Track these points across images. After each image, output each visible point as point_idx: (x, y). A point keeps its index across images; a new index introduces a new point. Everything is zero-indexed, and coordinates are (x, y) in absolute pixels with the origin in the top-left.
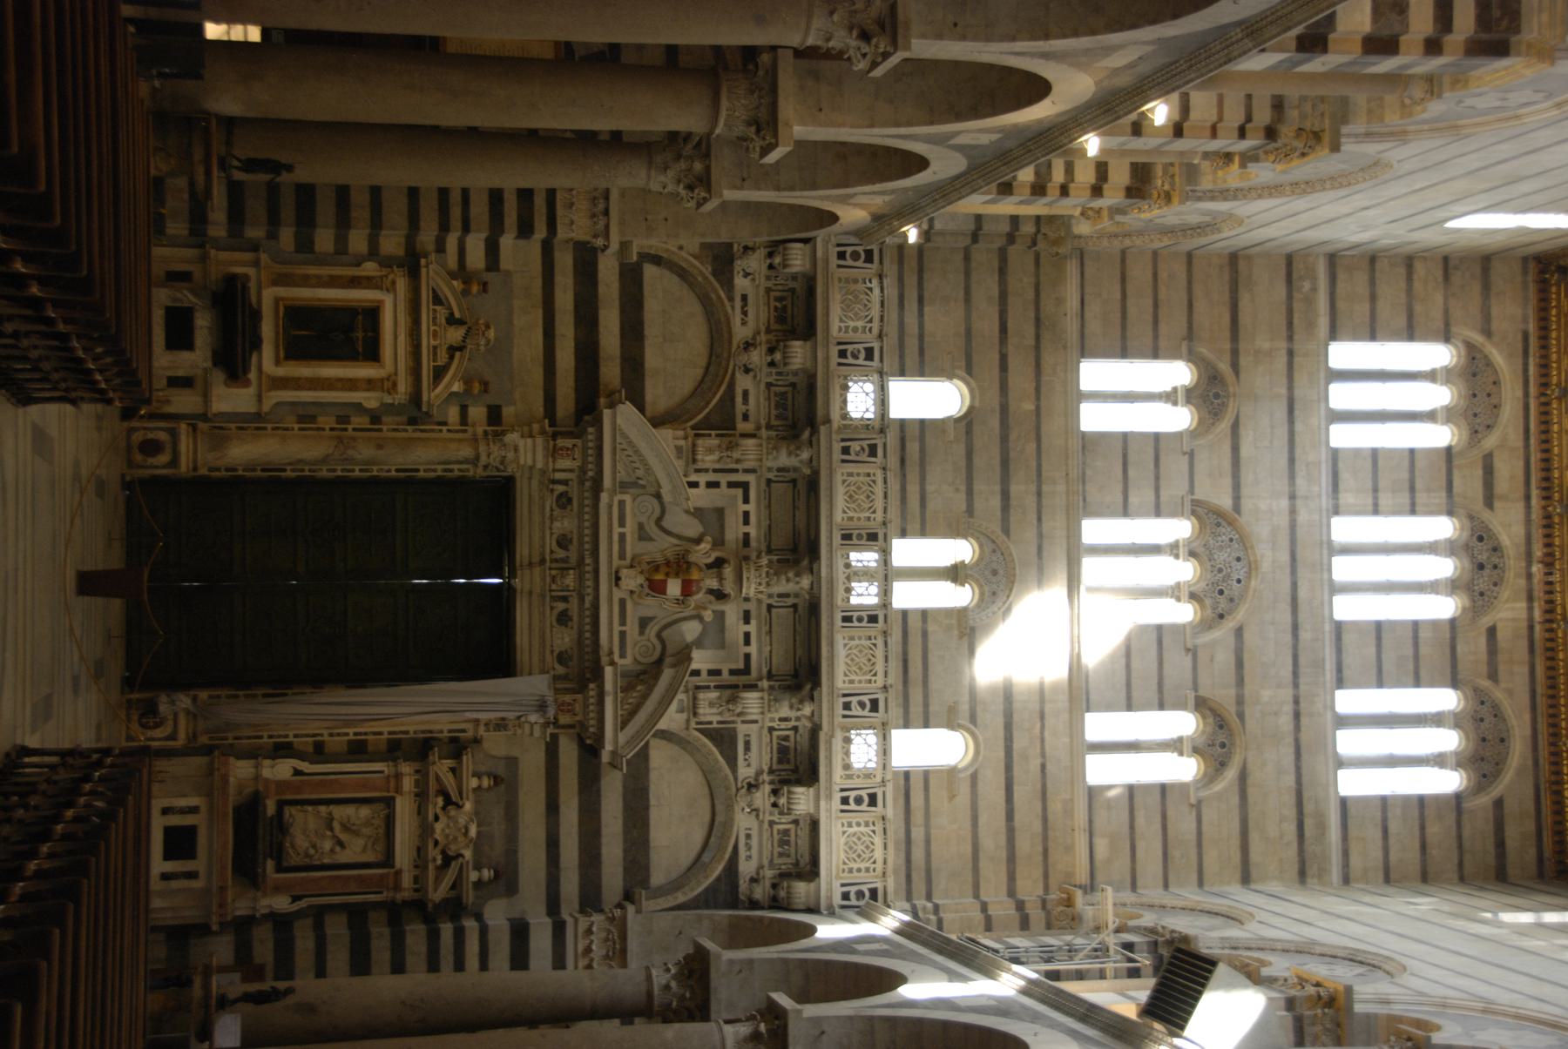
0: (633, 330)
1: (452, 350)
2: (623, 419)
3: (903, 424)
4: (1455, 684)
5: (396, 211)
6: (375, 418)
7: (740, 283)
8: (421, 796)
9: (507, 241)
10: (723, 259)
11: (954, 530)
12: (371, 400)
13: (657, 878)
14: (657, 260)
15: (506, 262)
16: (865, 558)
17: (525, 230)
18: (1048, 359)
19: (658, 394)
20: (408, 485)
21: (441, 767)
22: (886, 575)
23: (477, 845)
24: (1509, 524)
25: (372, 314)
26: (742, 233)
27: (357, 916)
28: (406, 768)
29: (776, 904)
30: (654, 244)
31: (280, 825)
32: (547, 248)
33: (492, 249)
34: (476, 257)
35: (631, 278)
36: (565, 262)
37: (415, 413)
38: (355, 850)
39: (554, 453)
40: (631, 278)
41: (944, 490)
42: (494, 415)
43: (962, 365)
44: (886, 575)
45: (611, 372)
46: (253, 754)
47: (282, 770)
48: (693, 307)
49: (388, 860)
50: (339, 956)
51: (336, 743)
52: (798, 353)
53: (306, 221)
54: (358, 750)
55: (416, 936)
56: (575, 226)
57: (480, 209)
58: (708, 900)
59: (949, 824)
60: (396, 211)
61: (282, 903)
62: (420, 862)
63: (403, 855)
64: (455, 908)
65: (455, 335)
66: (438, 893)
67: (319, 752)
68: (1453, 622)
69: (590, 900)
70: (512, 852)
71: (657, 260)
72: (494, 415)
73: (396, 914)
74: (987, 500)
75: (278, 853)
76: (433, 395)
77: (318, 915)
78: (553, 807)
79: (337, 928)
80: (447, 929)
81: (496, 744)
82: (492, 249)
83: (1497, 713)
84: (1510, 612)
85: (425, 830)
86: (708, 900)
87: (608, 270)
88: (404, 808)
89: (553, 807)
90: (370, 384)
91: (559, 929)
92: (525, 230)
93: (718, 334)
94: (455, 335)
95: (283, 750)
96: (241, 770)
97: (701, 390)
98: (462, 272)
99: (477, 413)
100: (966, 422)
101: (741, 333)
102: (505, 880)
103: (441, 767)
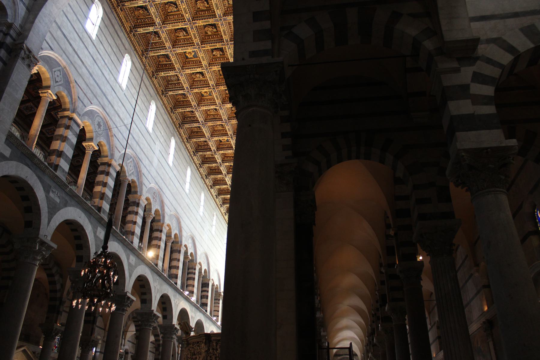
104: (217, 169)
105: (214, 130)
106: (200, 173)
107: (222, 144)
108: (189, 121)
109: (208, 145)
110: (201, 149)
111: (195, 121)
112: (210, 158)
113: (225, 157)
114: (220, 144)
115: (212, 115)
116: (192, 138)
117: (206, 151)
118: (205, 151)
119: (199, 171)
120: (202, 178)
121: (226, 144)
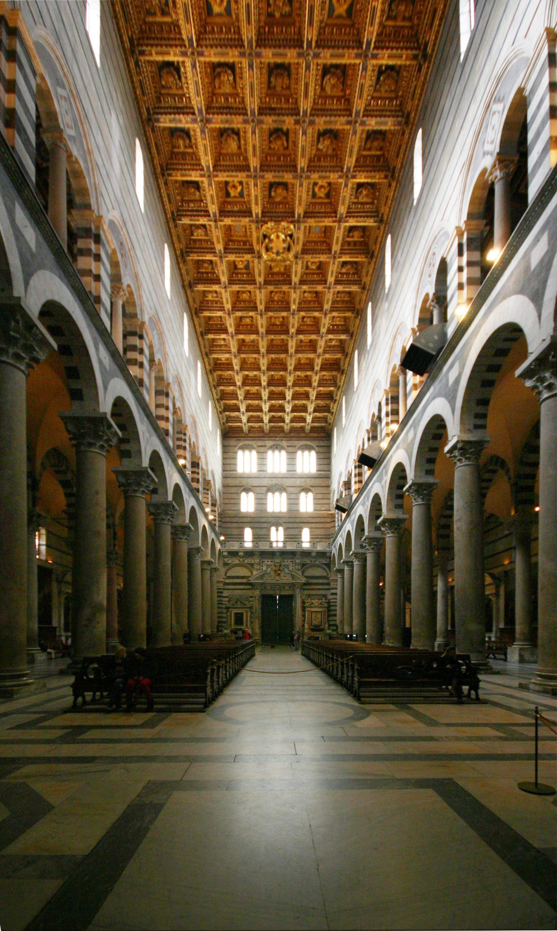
0: (238, 577)
1: (241, 603)
2: (252, 580)
3: (253, 538)
4: (296, 452)
5: (220, 610)
6: (252, 613)
7: (230, 562)
8: (311, 607)
9: (224, 595)
10: (225, 564)
11: (269, 530)
12: (249, 614)
13: (325, 575)
14: (226, 574)
15: (227, 595)
16: (274, 545)
17: (222, 592)
18: (241, 515)
19: (248, 574)
20: (263, 609)
21: (307, 605)
22: (277, 541)
23: (319, 599)
24: (269, 443)
25: (236, 614)
26: (221, 562)
27: (329, 616)
28: (307, 609)
29: (330, 558)
30: (223, 574)
31: (315, 626)
32: (224, 589)
33: (225, 597)
34: (227, 599)
35: (229, 577)
36: (226, 587)
37: (251, 608)
38: (319, 616)
39: (257, 589)
40: (229, 577)
41: (264, 532)
42: (251, 597)
43: (242, 529)
44: (277, 541)
45: (244, 581)
46: (304, 630)
47: (306, 626)
48: (233, 569)
49: (321, 612)
50: (334, 618)
51: (303, 618)
52: (240, 554)
53: (222, 622)
54: (304, 616)
55: (332, 608)
56: (221, 585)
57: (219, 599)
58: (329, 568)
59: (318, 532)
60: (220, 610)
61: (327, 626)
62: (321, 607)
63: (320, 610)
64: (329, 603)
65: (239, 603)
66: (326, 605)
67: (304, 621)
68: (287, 452)
69: (329, 584)
70: (320, 595)
71: (226, 574)
72: (251, 597)
73: (329, 611)
74: (265, 525)
75: (318, 626)
76: (248, 606)
77: (329, 621)
78: (314, 589)
79: (331, 618)
80: (332, 604)
81: (304, 597)
82: (225, 597)
83: (301, 446)
84: (284, 443)
85: (316, 607)
86: (329, 568)
87: (228, 581)
88: (313, 610)
89: (314, 589)
90: (247, 614)
91: (333, 589)
92: (222, 592)
93: (237, 565)
94: (239, 603)
95: (303, 626)
96: (306, 631)
97: (247, 567)
98: (229, 601)
99: (251, 599)
100: (252, 528)
101: (237, 562)
102: (325, 596)
103: (307, 605)
104: (209, 273)
105: (221, 154)
106: (181, 275)
107: (230, 203)
108: (171, 108)
109: (202, 201)
110: (188, 211)
111: (183, 108)
112: (200, 240)
113: (230, 240)
114: (226, 202)
115: (223, 95)
116: (174, 170)
117: (198, 216)
118: (195, 216)
119: (180, 269)
120: (183, 286)
121: (238, 202)
